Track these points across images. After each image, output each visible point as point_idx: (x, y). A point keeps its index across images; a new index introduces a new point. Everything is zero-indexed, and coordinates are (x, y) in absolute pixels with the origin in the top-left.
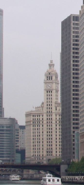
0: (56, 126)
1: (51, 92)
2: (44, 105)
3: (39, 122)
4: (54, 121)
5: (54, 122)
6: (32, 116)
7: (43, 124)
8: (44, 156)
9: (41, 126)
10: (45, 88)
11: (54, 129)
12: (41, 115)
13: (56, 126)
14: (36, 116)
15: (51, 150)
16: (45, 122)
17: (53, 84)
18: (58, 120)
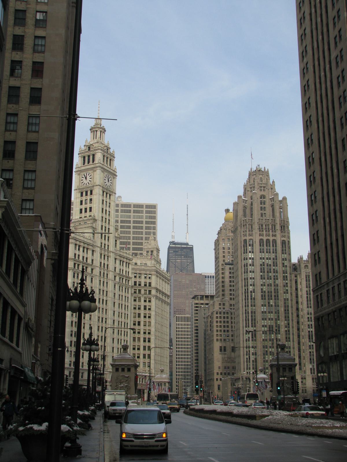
2: (96, 225)
4: (113, 273)
6: (74, 246)
11: (110, 295)
14: (81, 249)
16: (96, 271)
17: (114, 178)
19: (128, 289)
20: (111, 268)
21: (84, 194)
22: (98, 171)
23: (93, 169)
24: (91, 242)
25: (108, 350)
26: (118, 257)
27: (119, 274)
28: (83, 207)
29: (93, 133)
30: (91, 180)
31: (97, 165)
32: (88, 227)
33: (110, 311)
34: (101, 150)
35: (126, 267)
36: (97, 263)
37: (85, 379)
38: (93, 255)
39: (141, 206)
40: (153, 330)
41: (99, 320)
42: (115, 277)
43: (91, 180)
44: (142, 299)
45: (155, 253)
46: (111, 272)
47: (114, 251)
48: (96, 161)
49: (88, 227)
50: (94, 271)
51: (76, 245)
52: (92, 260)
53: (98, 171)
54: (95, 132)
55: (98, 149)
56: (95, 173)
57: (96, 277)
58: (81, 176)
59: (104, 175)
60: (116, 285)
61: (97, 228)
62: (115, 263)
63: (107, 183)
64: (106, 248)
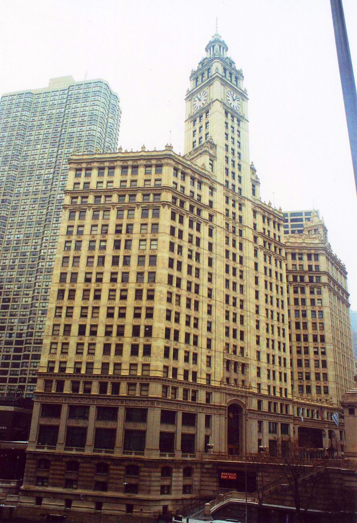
0: (256, 255)
1: (239, 125)
2: (215, 153)
3: (199, 211)
4: (251, 231)
5: (248, 234)
7: (210, 224)
8: (213, 384)
9: (205, 229)
10: (222, 97)
11: (249, 263)
12: (206, 184)
13: (256, 255)
14: (188, 179)
15: (241, 360)
16: (219, 220)
17: (243, 100)
18: (260, 233)
19: (280, 262)
20: (246, 223)
21: (198, 120)
22: (217, 83)
23: (210, 83)
24: (207, 173)
25: (247, 355)
26: (257, 209)
27: (263, 234)
28: (197, 138)
29: (209, 50)
30: (206, 98)
31: (213, 77)
32: (201, 154)
33: (248, 289)
34: (221, 60)
35: (274, 227)
36: (220, 205)
37: (200, 404)
38: (211, 194)
39: (301, 214)
40: (328, 335)
41: (227, 302)
42: (255, 238)
43: (206, 98)
44: (307, 290)
45: (321, 230)
46: (247, 229)
47: (250, 198)
48: (213, 71)
49: (201, 154)
50: (215, 218)
51: (176, 169)
52: (211, 202)
53: (217, 83)
54: (212, 48)
55: (215, 58)
56: (212, 87)
57: (219, 229)
58: (193, 100)
59: (226, 91)
60: (259, 251)
61: (218, 157)
62: (255, 216)
63: (231, 101)
64: (237, 191)
